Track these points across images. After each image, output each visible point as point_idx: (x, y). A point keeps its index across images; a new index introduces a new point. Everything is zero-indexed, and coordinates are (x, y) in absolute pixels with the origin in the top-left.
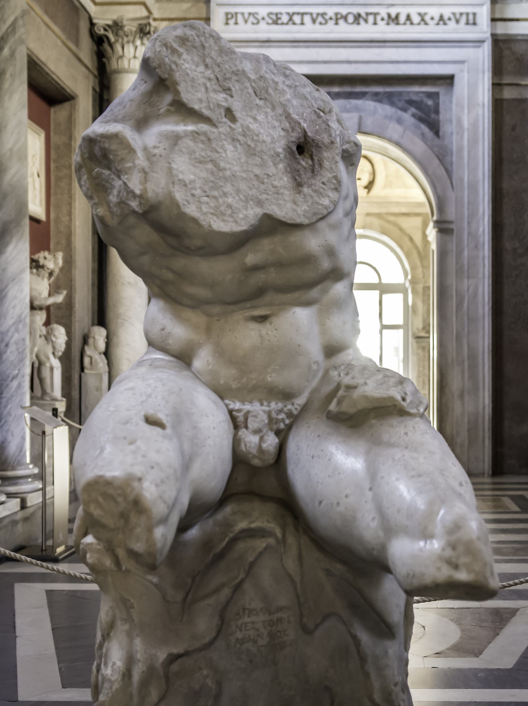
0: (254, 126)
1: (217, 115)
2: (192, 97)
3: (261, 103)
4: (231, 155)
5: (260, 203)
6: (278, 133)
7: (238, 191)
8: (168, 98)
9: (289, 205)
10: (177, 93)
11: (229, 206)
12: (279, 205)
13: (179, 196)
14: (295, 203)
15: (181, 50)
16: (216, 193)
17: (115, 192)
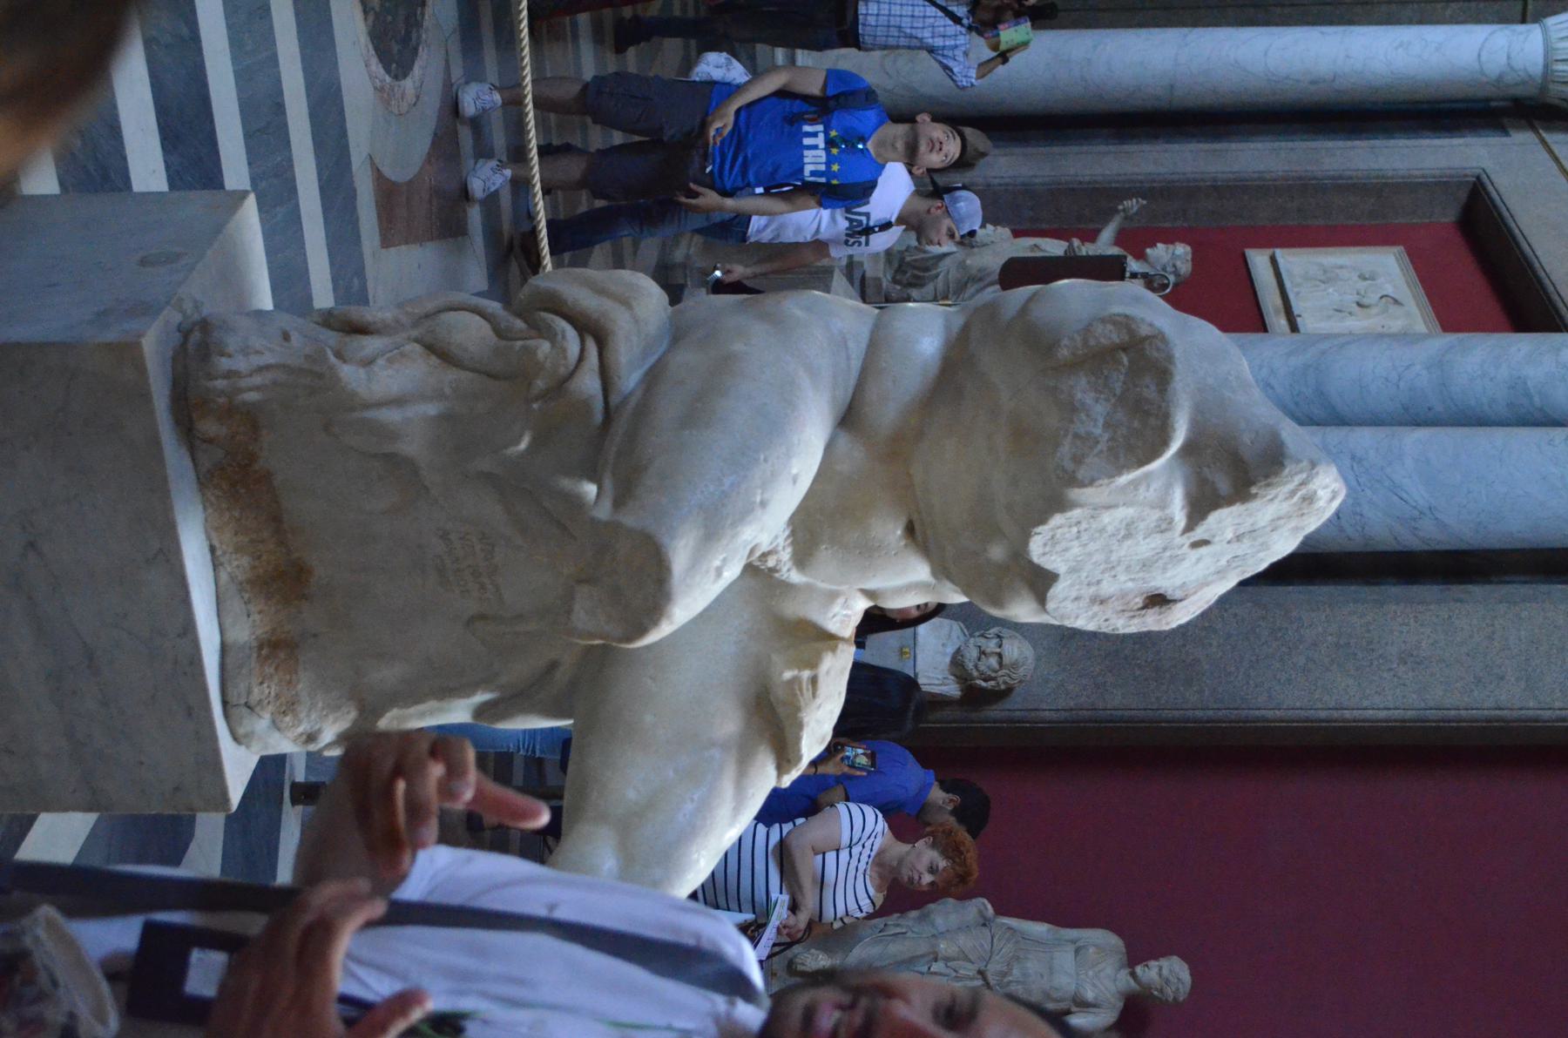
0: (1186, 564)
1: (1200, 533)
2: (1223, 521)
3: (1223, 562)
4: (1145, 547)
5: (1073, 570)
6: (1178, 582)
7: (1090, 555)
8: (1224, 485)
9: (1074, 594)
10: (1230, 502)
11: (1066, 550)
12: (1072, 585)
13: (1076, 513)
14: (1077, 599)
15: (1296, 499)
16: (1085, 537)
17: (1089, 398)
